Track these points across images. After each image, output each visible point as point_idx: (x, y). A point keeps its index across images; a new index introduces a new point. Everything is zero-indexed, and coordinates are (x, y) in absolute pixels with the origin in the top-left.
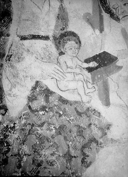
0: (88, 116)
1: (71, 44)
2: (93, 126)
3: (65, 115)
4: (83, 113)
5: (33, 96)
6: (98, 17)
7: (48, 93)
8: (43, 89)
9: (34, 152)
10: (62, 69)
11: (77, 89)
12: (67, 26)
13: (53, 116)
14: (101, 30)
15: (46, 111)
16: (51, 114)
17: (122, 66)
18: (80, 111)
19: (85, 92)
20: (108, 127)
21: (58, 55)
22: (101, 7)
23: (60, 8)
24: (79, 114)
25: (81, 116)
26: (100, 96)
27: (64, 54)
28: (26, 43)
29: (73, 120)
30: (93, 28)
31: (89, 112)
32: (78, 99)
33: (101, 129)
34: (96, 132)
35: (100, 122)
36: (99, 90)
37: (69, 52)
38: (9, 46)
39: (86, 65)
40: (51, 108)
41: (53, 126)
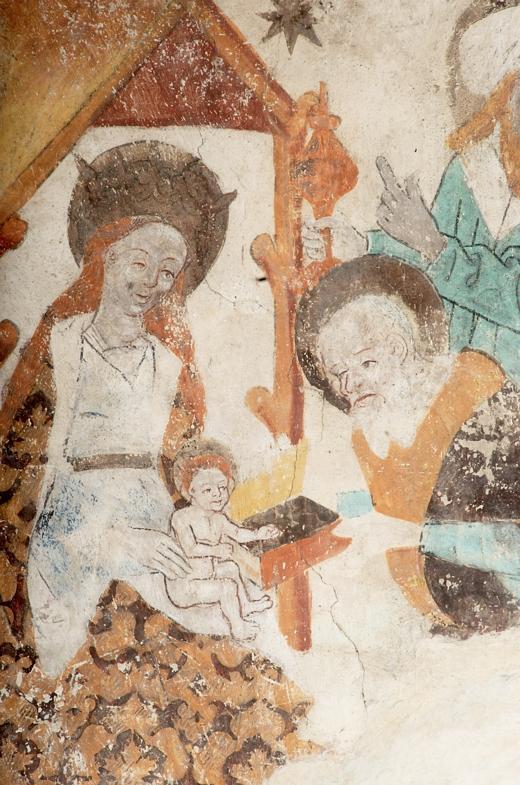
0: (247, 679)
1: (208, 478)
2: (259, 705)
3: (183, 674)
4: (235, 669)
5: (102, 621)
6: (290, 397)
7: (142, 612)
8: (129, 603)
9: (101, 770)
10: (180, 546)
11: (219, 602)
12: (202, 424)
13: (153, 676)
14: (296, 436)
15: (135, 660)
16: (149, 670)
17: (350, 539)
18: (225, 662)
19: (241, 613)
20: (302, 709)
21: (172, 507)
22: (300, 368)
23: (183, 379)
24: (223, 671)
25: (229, 679)
26: (283, 622)
27: (189, 504)
28: (91, 478)
29: (205, 687)
30: (274, 431)
31: (246, 667)
32: (221, 628)
33: (283, 713)
34: (265, 722)
35: (281, 694)
36: (282, 605)
37: (202, 499)
38: (44, 490)
39: (247, 536)
40: (149, 653)
41: (152, 704)
